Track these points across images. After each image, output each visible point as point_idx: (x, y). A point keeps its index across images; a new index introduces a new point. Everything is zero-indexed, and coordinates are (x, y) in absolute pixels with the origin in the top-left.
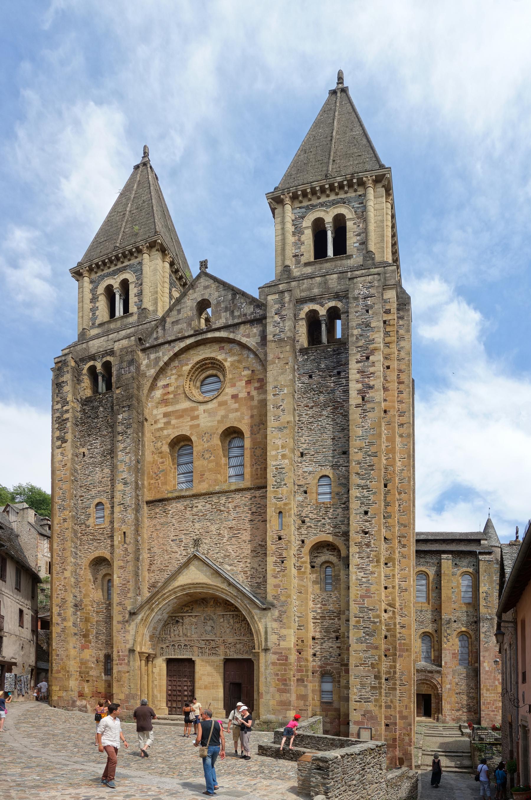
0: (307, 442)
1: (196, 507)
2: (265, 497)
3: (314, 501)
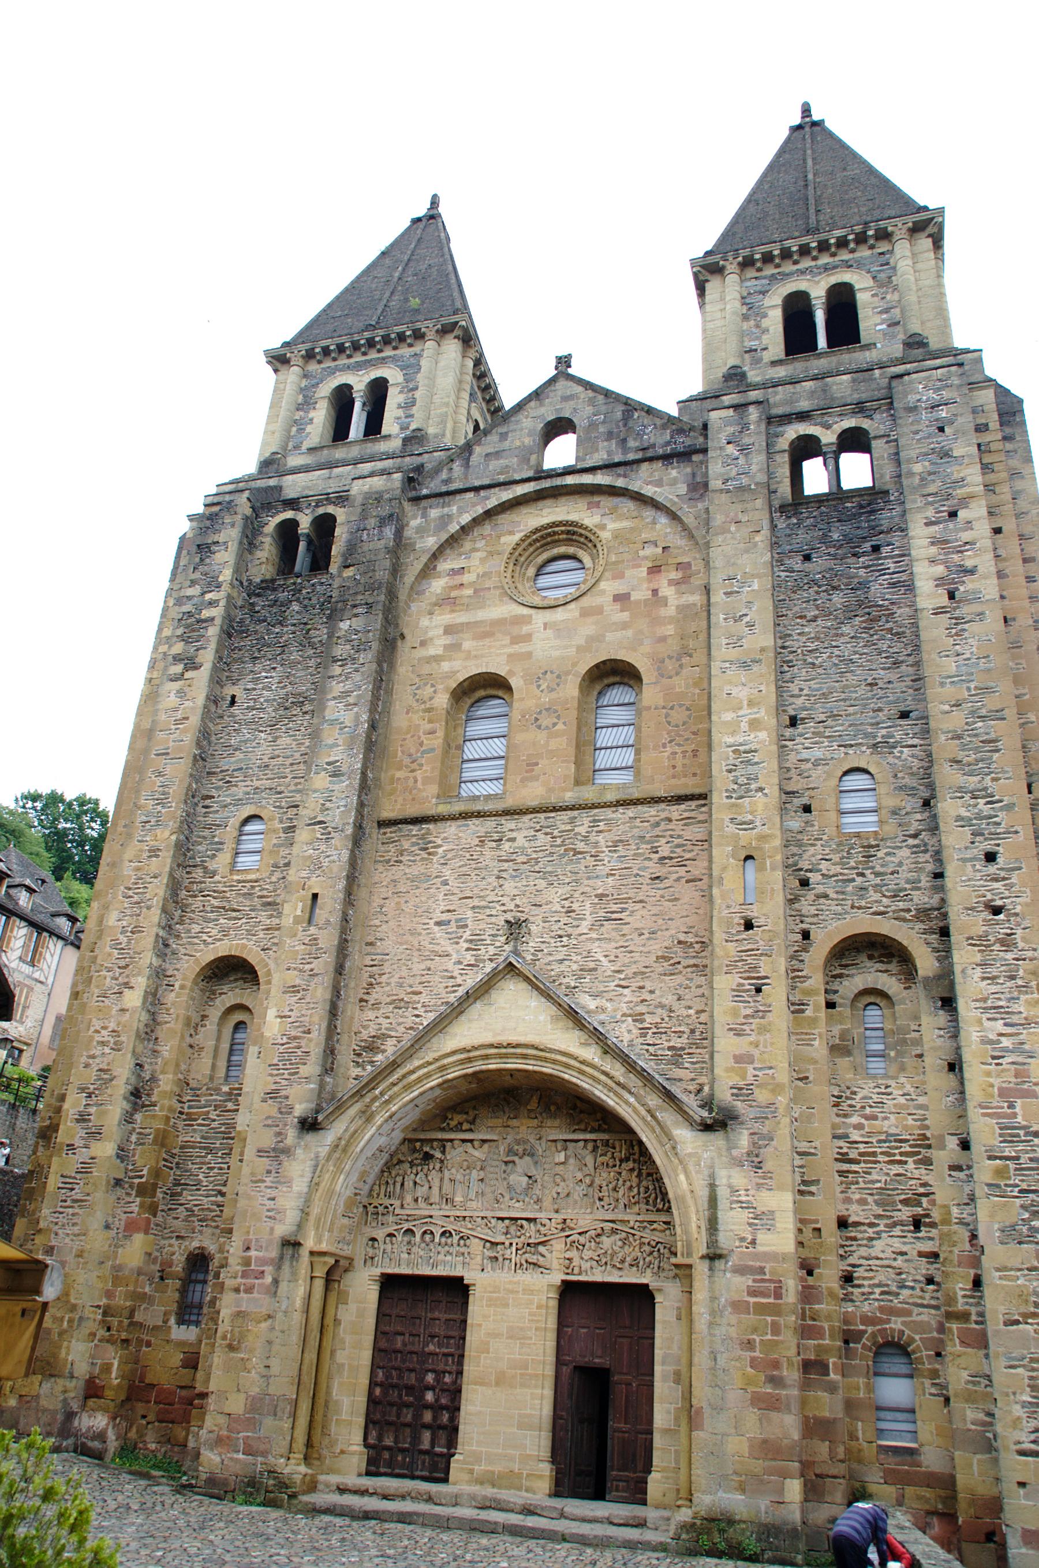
0: (805, 692)
1: (509, 840)
3: (831, 831)
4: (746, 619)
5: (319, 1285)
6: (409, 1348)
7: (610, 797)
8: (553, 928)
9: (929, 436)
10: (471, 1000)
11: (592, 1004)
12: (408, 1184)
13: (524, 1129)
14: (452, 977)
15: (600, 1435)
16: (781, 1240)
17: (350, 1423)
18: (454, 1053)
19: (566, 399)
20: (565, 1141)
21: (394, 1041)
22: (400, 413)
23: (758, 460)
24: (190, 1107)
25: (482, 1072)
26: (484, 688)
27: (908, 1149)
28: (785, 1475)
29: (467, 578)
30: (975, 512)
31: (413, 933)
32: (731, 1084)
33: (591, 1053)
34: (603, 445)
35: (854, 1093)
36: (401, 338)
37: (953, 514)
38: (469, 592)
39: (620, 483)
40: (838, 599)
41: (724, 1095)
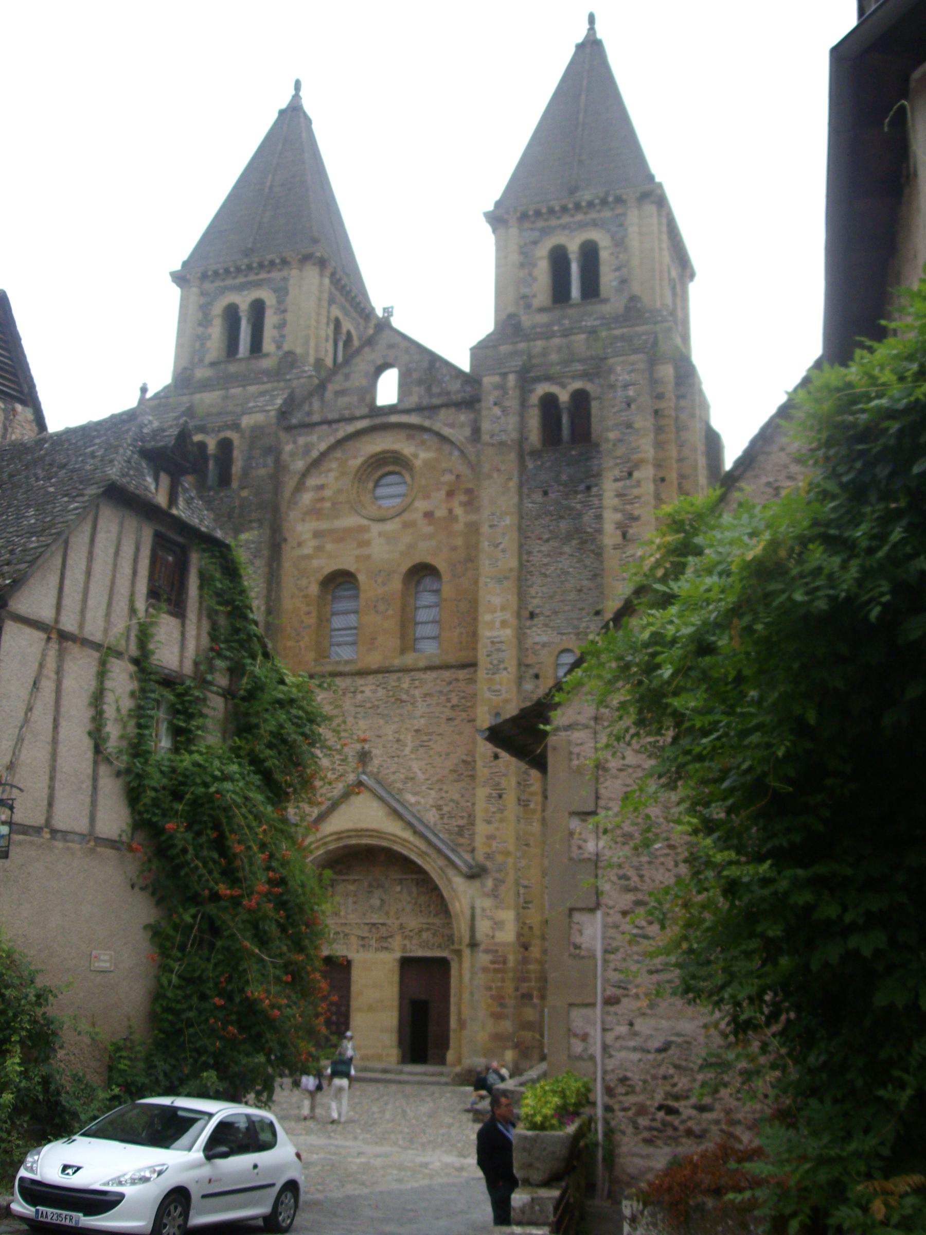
2: (472, 681)
4: (502, 546)
7: (422, 664)
9: (621, 411)
11: (412, 799)
16: (508, 935)
18: (331, 835)
19: (391, 346)
22: (275, 333)
23: (512, 422)
26: (340, 581)
28: (505, 1048)
29: (327, 493)
30: (646, 473)
33: (407, 835)
34: (415, 389)
36: (272, 263)
37: (630, 474)
38: (328, 504)
39: (427, 423)
40: (564, 526)
41: (480, 857)
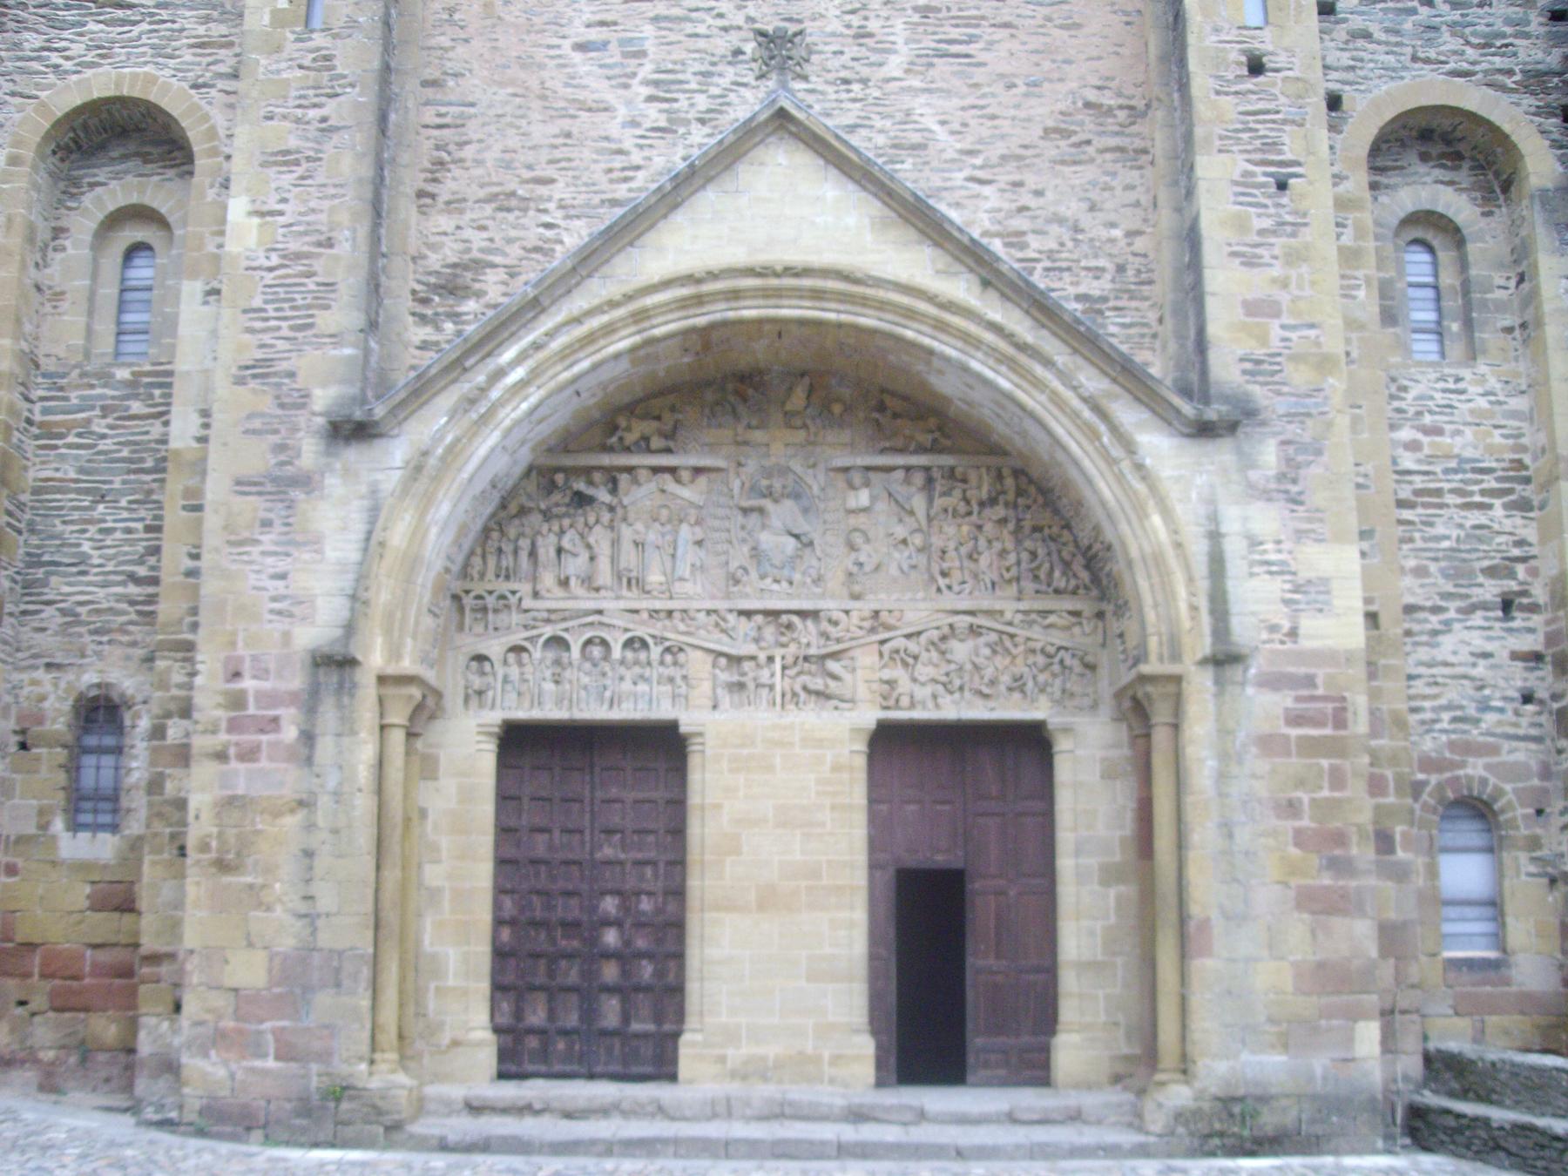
5: (397, 738)
6: (560, 856)
8: (829, 65)
10: (698, 181)
12: (546, 550)
13: (778, 447)
14: (620, 152)
15: (950, 980)
16: (1338, 629)
17: (465, 992)
18: (666, 284)
20: (868, 469)
21: (501, 274)
24: (45, 411)
25: (725, 324)
27: (1495, 485)
28: (1354, 1015)
31: (526, 63)
32: (1240, 352)
33: (961, 288)
35: (1405, 389)
